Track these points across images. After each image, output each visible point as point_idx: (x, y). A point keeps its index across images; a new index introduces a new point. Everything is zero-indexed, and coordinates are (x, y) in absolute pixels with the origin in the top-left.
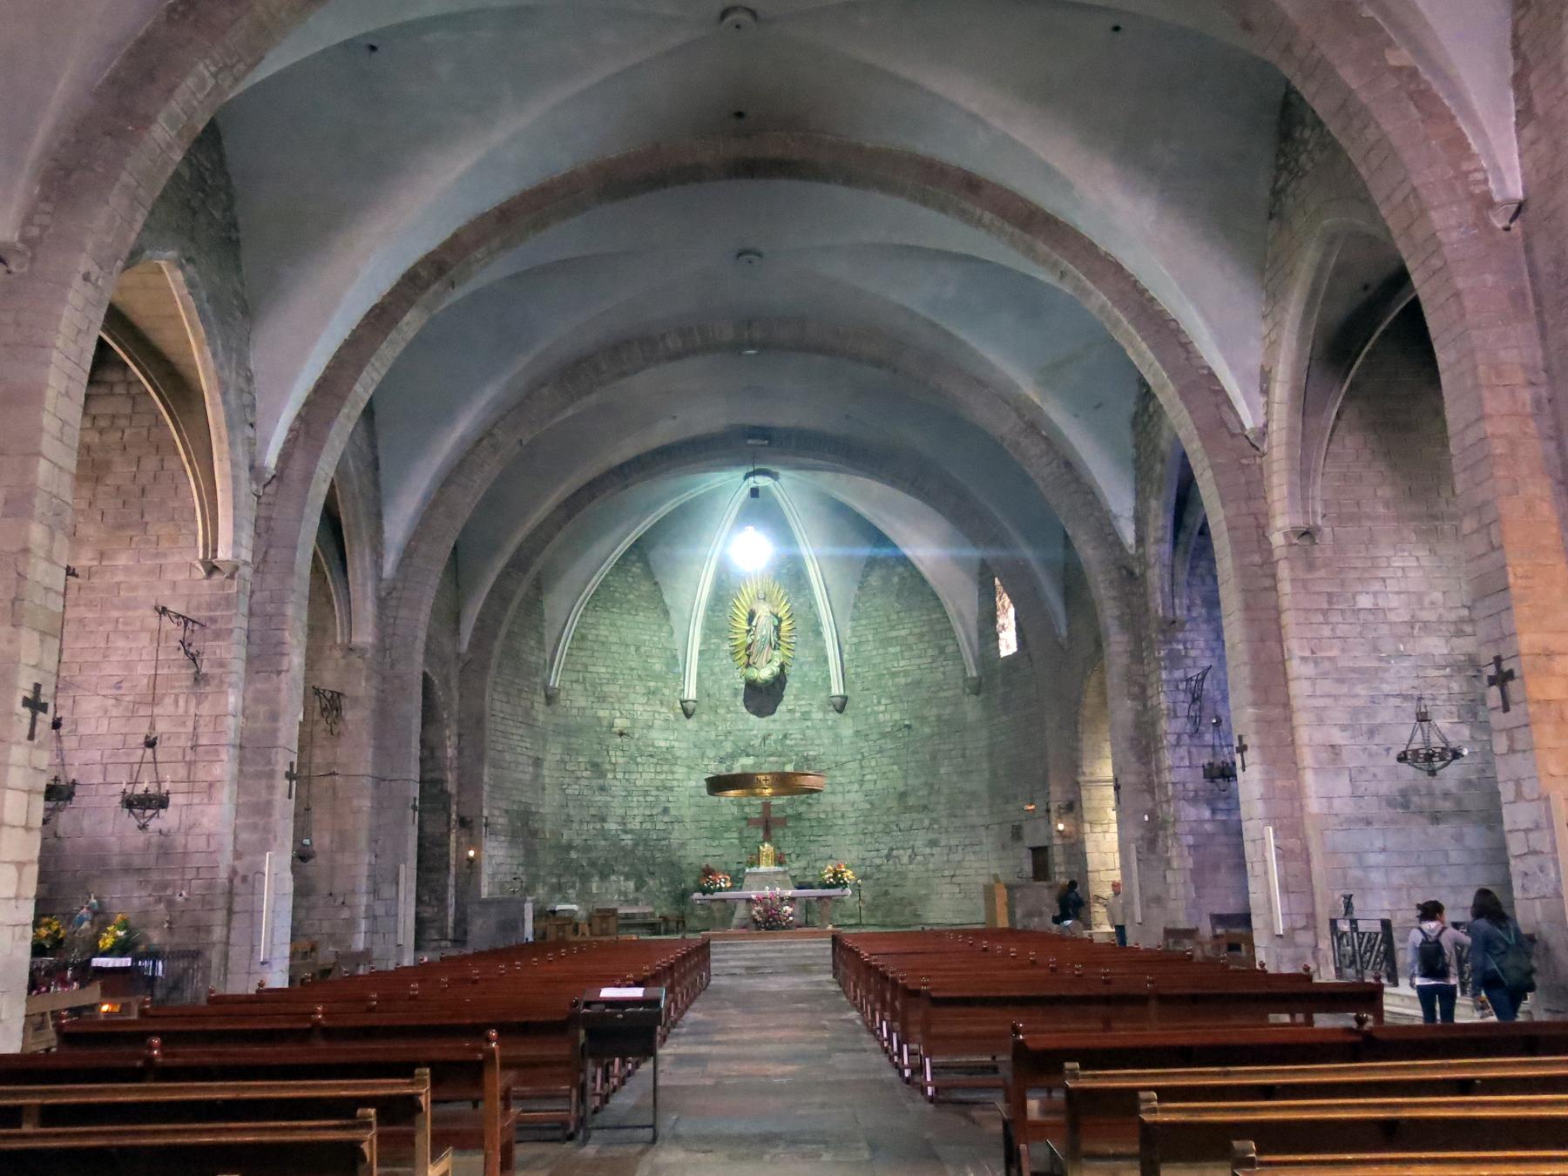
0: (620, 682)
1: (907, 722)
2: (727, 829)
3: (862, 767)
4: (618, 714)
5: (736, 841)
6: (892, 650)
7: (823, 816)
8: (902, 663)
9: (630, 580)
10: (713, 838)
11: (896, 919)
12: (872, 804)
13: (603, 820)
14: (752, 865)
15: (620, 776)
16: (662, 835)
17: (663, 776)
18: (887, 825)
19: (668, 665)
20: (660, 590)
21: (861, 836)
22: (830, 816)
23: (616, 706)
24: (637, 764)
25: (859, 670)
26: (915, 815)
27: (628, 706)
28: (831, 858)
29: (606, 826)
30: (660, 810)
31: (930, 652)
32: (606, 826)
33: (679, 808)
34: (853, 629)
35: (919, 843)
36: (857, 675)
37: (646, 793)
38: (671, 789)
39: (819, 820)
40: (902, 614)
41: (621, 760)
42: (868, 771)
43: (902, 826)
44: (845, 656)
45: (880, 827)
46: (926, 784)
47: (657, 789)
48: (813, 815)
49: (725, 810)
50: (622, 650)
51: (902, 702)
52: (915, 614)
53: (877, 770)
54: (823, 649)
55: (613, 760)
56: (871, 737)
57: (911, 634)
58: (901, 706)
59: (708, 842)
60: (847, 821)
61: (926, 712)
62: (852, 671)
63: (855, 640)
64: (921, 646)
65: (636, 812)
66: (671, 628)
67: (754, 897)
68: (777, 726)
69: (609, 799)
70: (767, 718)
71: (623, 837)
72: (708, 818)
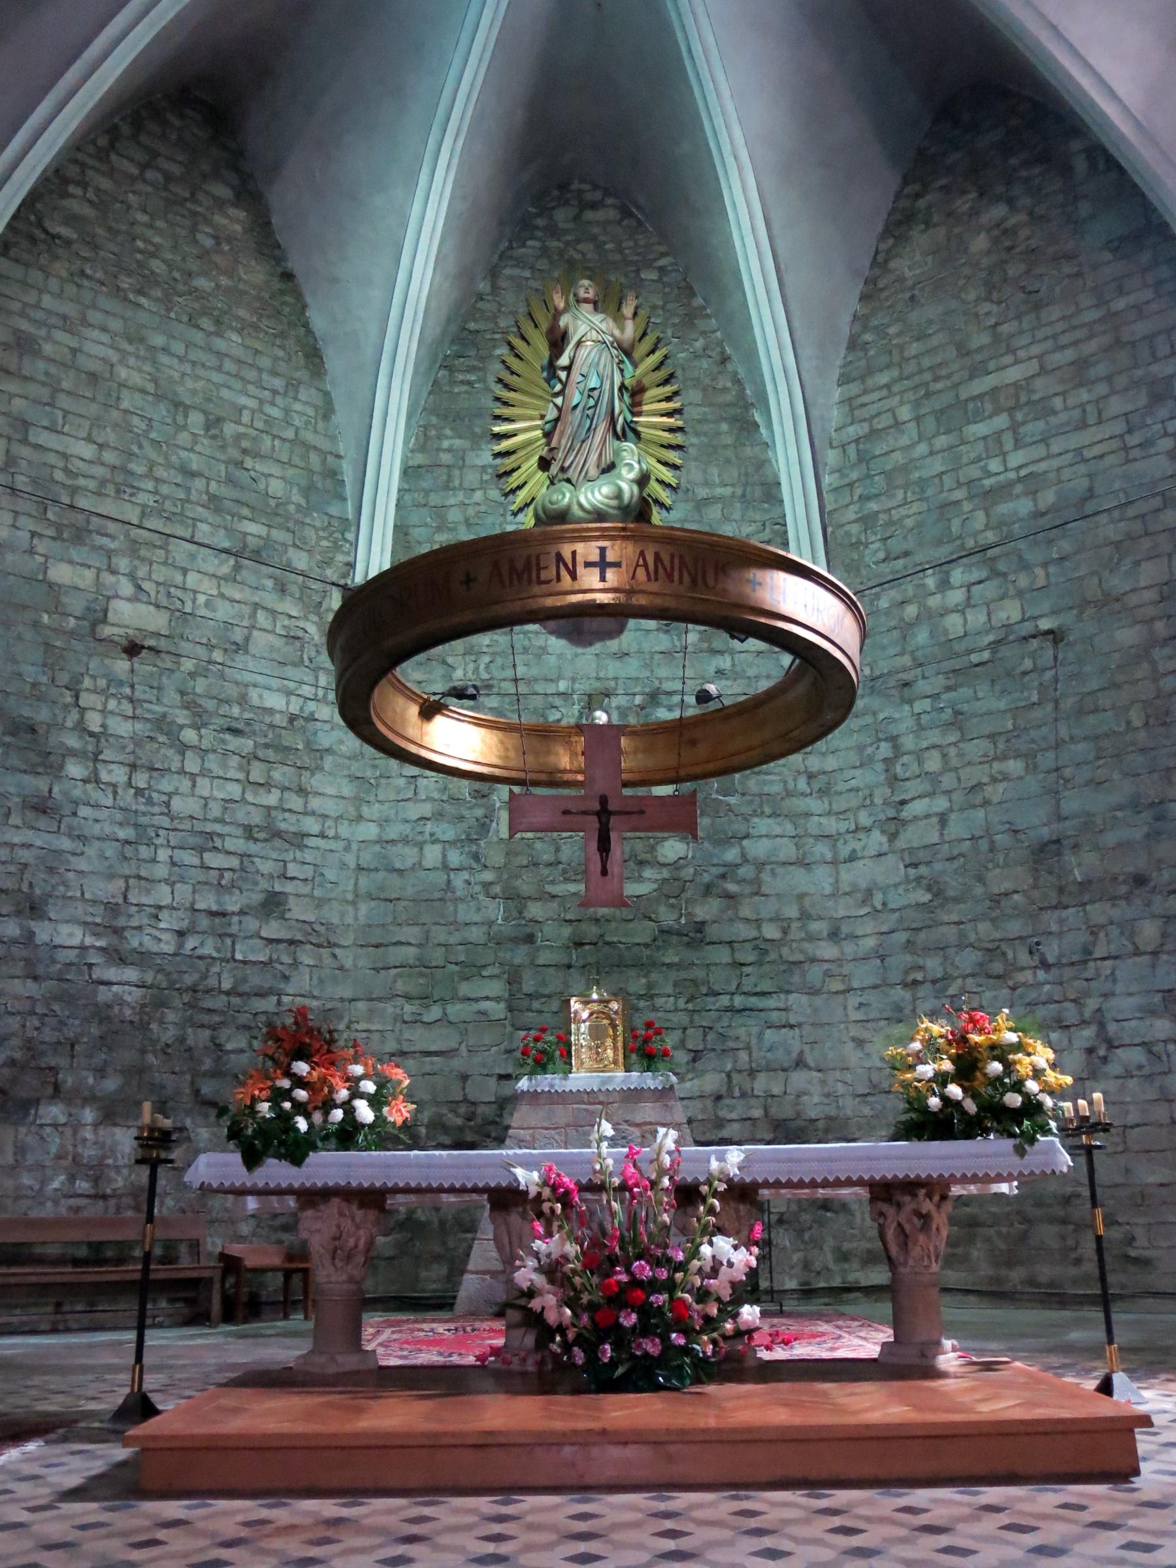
0: (142, 498)
1: (1045, 624)
2: (471, 970)
3: (893, 780)
4: (126, 588)
5: (497, 1009)
6: (980, 429)
7: (771, 932)
8: (1015, 459)
9: (208, 243)
10: (425, 999)
11: (1045, 1272)
12: (935, 888)
13: (34, 909)
14: (541, 1064)
15: (118, 775)
16: (257, 979)
17: (272, 799)
18: (993, 951)
19: (308, 490)
20: (299, 296)
21: (899, 993)
22: (795, 933)
23: (123, 564)
24: (183, 748)
25: (874, 506)
26: (1099, 912)
27: (161, 573)
28: (800, 1063)
29: (43, 932)
30: (257, 898)
31: (1116, 405)
32: (43, 932)
33: (320, 903)
34: (849, 402)
35: (1123, 1004)
36: (867, 521)
37: (207, 842)
38: (298, 840)
39: (762, 947)
40: (1005, 329)
41: (122, 728)
42: (913, 788)
43: (1051, 950)
44: (827, 480)
45: (968, 959)
46: (1135, 805)
47: (249, 832)
48: (744, 931)
49: (465, 913)
50: (162, 411)
51: (1025, 566)
52: (1055, 312)
53: (948, 781)
54: (762, 464)
55: (94, 722)
56: (922, 686)
57: (1043, 371)
58: (1023, 581)
59: (409, 1009)
60: (849, 949)
61: (1117, 583)
62: (851, 514)
63: (853, 431)
64: (1084, 395)
65: (163, 895)
66: (327, 395)
67: (527, 1178)
68: (632, 668)
69: (66, 844)
70: (598, 647)
71: (111, 974)
72: (411, 933)
